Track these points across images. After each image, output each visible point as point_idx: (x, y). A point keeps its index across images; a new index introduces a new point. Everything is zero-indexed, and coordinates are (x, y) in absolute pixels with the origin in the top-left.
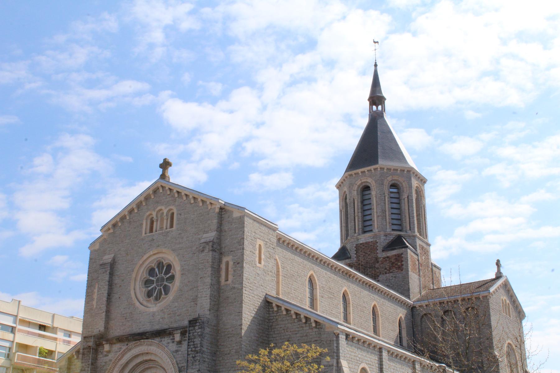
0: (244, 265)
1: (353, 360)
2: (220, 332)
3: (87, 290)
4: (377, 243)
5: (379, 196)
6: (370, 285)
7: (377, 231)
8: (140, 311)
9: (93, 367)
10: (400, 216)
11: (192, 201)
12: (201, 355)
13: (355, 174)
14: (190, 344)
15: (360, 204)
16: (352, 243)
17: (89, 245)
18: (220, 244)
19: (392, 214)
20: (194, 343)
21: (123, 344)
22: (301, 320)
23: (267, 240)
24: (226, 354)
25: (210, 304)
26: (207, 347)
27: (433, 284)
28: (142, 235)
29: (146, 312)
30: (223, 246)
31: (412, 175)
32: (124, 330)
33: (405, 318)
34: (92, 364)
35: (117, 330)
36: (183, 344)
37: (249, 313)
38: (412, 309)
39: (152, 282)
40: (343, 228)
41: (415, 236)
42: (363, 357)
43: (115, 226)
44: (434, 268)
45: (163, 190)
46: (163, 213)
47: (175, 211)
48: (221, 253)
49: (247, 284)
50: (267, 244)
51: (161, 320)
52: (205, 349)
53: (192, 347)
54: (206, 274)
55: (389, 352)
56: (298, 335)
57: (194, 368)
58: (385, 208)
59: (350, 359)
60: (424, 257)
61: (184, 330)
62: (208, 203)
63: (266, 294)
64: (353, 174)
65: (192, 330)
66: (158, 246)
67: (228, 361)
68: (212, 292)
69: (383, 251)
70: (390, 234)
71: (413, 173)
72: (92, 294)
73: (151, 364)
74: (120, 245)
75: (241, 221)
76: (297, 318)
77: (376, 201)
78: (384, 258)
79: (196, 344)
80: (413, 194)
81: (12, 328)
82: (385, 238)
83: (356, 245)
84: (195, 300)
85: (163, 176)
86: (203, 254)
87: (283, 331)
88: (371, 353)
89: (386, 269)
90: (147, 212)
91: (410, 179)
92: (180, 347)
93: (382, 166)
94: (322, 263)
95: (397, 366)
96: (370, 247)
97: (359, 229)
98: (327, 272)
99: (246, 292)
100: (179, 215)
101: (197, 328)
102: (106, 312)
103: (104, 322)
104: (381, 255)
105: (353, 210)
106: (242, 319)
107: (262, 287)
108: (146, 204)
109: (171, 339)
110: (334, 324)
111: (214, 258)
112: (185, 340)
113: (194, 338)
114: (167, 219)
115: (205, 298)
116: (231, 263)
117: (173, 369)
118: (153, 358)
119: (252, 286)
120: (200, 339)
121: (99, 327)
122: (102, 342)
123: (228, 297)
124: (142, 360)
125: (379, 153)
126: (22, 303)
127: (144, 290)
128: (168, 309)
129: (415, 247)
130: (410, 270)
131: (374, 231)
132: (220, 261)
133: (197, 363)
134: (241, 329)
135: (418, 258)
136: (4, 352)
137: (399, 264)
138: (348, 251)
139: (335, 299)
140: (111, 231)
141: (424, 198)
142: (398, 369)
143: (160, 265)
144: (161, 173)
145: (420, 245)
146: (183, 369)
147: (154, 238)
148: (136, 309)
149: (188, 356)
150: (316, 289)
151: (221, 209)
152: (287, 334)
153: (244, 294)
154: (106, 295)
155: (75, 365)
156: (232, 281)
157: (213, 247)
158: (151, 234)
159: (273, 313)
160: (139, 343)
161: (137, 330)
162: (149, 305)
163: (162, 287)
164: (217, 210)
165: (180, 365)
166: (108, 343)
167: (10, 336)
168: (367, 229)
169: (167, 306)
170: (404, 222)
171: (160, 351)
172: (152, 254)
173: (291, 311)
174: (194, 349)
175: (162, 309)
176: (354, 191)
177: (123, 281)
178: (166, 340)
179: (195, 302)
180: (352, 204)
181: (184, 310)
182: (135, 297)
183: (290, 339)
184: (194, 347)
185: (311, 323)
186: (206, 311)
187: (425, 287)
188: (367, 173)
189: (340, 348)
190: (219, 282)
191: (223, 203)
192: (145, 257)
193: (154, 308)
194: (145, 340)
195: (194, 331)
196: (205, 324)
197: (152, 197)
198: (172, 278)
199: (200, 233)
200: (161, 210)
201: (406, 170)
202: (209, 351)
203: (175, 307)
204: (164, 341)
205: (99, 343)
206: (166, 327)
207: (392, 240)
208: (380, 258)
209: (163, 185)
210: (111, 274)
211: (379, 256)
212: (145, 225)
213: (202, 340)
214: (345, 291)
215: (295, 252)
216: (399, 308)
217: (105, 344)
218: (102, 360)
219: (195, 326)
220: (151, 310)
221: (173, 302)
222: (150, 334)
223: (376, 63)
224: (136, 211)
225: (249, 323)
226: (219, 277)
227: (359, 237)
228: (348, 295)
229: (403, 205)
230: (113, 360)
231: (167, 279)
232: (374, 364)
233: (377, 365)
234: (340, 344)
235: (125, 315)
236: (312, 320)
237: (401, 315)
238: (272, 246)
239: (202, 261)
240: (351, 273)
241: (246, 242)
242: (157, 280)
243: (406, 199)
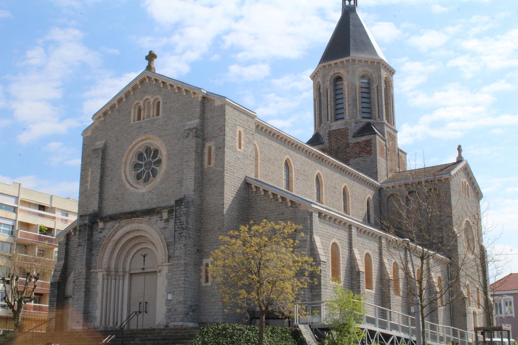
0: (226, 150)
1: (325, 236)
2: (204, 211)
3: (81, 173)
4: (348, 129)
5: (351, 86)
6: (341, 169)
7: (348, 118)
9: (89, 242)
10: (369, 104)
11: (177, 91)
12: (187, 231)
13: (328, 65)
14: (177, 221)
15: (332, 94)
16: (325, 129)
17: (81, 132)
18: (203, 131)
19: (362, 102)
21: (115, 222)
22: (277, 200)
23: (247, 127)
24: (209, 231)
25: (195, 185)
26: (192, 224)
27: (399, 167)
28: (130, 122)
30: (206, 132)
31: (382, 66)
32: (116, 209)
33: (373, 198)
34: (88, 240)
35: (110, 210)
37: (230, 194)
38: (380, 190)
39: (141, 166)
40: (317, 115)
41: (383, 124)
42: (333, 233)
43: (105, 114)
44: (400, 153)
45: (149, 81)
46: (150, 102)
47: (161, 100)
48: (204, 139)
49: (228, 167)
50: (246, 131)
51: (150, 200)
52: (190, 226)
53: (178, 224)
54: (190, 158)
55: (357, 228)
56: (275, 213)
58: (356, 97)
59: (323, 235)
60: (391, 143)
61: (171, 209)
62: (191, 92)
63: (246, 176)
64: (326, 65)
65: (178, 209)
66: (146, 133)
67: (211, 237)
68: (196, 175)
69: (354, 137)
70: (360, 122)
71: (383, 64)
72: (86, 177)
73: (142, 240)
74: (111, 132)
75: (222, 109)
76: (274, 198)
77: (348, 91)
78: (354, 144)
80: (382, 84)
81: (15, 208)
82: (355, 125)
83: (329, 131)
84: (180, 182)
85: (149, 68)
86: (187, 140)
87: (261, 210)
88: (342, 229)
89: (356, 153)
90: (135, 101)
91: (380, 70)
92: (167, 224)
93: (354, 58)
94: (297, 148)
95: (365, 241)
96: (342, 133)
97: (331, 117)
98: (302, 156)
99: (228, 175)
100: (164, 104)
101: (182, 207)
102: (99, 193)
103: (98, 202)
104: (352, 141)
105: (326, 100)
106: (224, 199)
107: (242, 170)
108: (134, 94)
110: (308, 203)
111: (197, 144)
112: (172, 218)
113: (180, 217)
114: (154, 108)
115: (190, 180)
116: (213, 148)
117: (161, 244)
118: (143, 234)
119: (233, 169)
120: (185, 217)
121: (94, 207)
123: (211, 179)
124: (133, 236)
125: (351, 46)
126: (22, 186)
127: (133, 173)
129: (383, 133)
130: (378, 154)
131: (345, 119)
132: (203, 146)
133: (184, 238)
134: (223, 208)
135: (386, 143)
136: (8, 229)
137: (368, 149)
138: (321, 136)
139: (309, 181)
140: (102, 119)
141: (393, 88)
142: (366, 244)
143: (148, 150)
144: (147, 65)
145: (388, 131)
147: (142, 125)
149: (176, 233)
150: (292, 171)
151: (204, 98)
152: (265, 212)
153: (225, 177)
154: (99, 177)
155: (72, 241)
156: (215, 165)
157: (196, 133)
158: (139, 121)
159: (252, 194)
162: (139, 187)
163: (150, 170)
164: (200, 99)
165: (168, 241)
167: (13, 216)
168: (339, 116)
170: (373, 110)
171: (150, 228)
172: (140, 140)
173: (268, 191)
174: (180, 226)
176: (327, 81)
177: (114, 165)
178: (155, 218)
179: (181, 184)
180: (326, 93)
181: (171, 191)
182: (125, 179)
183: (268, 217)
185: (287, 203)
187: (391, 170)
188: (339, 64)
189: (313, 225)
190: (202, 166)
191: (206, 92)
192: (134, 143)
193: (143, 189)
195: (180, 210)
196: (191, 204)
197: (140, 87)
198: (159, 162)
199: (184, 121)
200: (148, 99)
201: (376, 62)
202: (194, 228)
203: (163, 188)
206: (154, 206)
207: (362, 127)
208: (351, 143)
209: (149, 76)
210: (103, 159)
211: (350, 141)
212: (133, 114)
213: (187, 218)
214: (319, 173)
215: (272, 138)
216: (367, 189)
218: (97, 236)
220: (141, 191)
221: (161, 184)
224: (124, 100)
225: (230, 203)
226: (202, 160)
227: (332, 124)
228: (321, 178)
229: (372, 95)
230: (107, 236)
231: (154, 162)
232: (344, 239)
233: (347, 240)
234: (314, 222)
235: (117, 196)
236: (288, 200)
237: (369, 195)
238: (251, 132)
239: (187, 146)
240: (324, 157)
241: (227, 129)
242: (146, 164)
243: (376, 89)
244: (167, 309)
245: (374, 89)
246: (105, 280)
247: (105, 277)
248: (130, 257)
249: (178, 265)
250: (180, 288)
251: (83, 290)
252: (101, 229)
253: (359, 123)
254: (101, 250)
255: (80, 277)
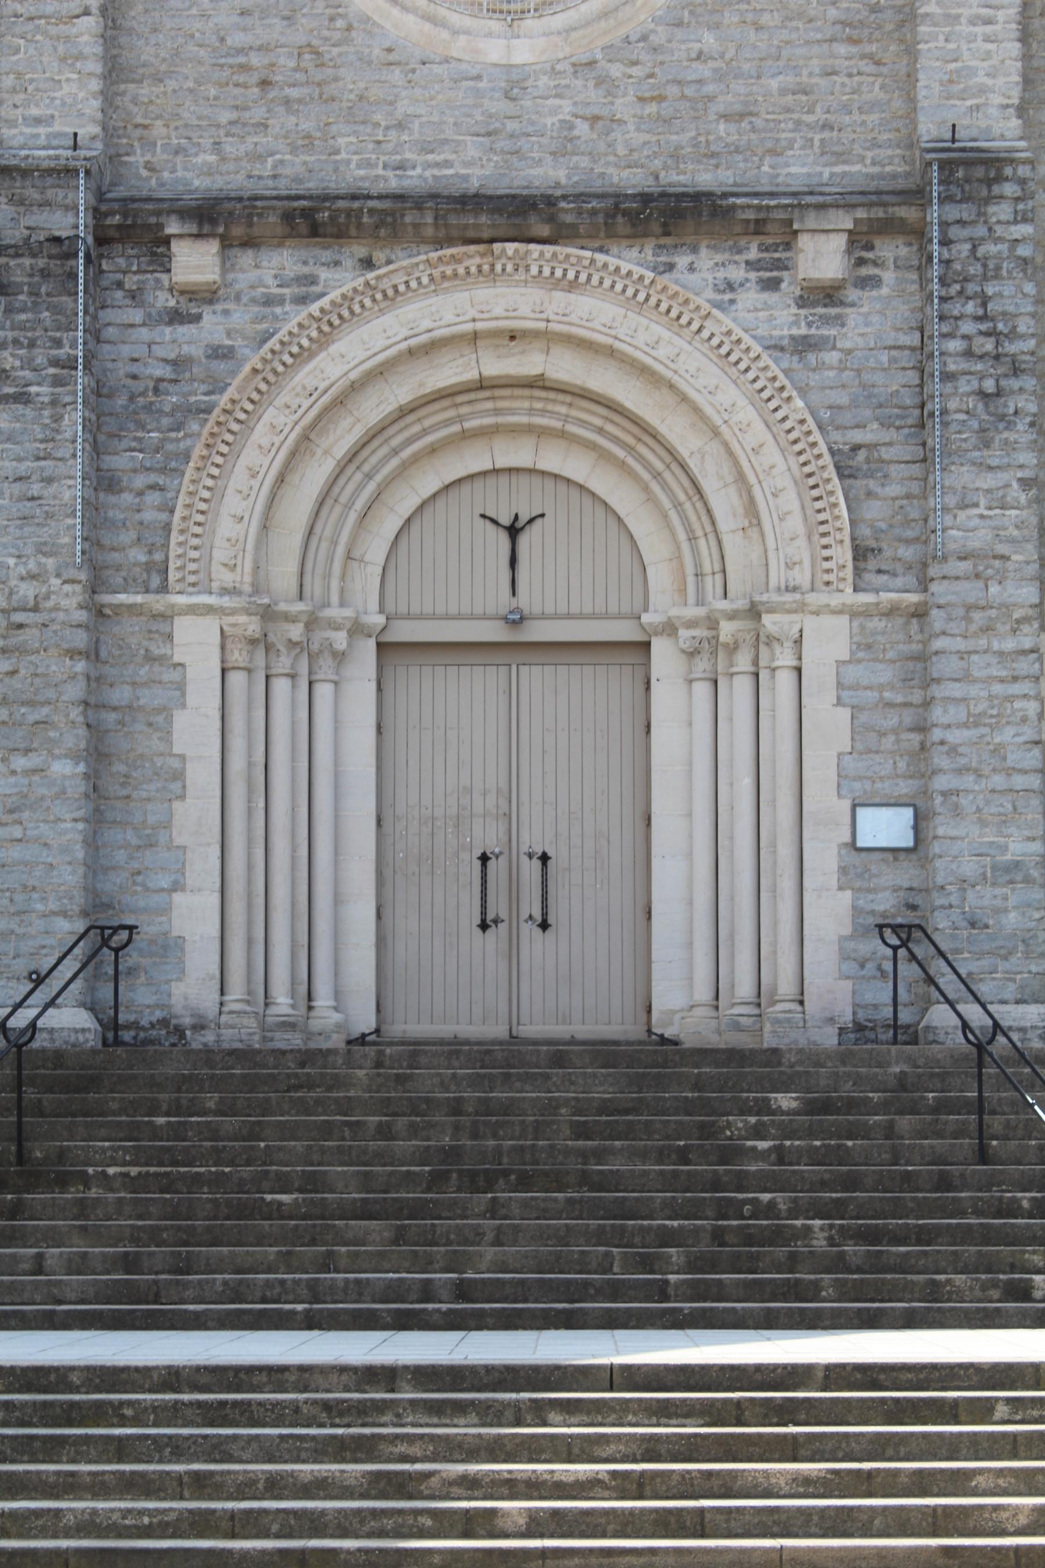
8: (389, 50)
20: (984, 305)
21: (326, 255)
29: (447, 60)
36: (853, 305)
51: (582, 128)
53: (968, 327)
57: (995, 462)
79: (1004, 314)
92: (826, 320)
101: (1002, 211)
109: (747, 263)
113: (985, 278)
115: (980, 30)
122: (153, 220)
128: (635, 63)
146: (868, 461)
148: (349, 28)
160: (477, 260)
161: (380, 171)
166: (212, 235)
169: (627, 40)
175: (584, 58)
181: (774, 84)
184: (987, 334)
186: (993, 111)
194: (532, 246)
195: (981, 231)
204: (691, 268)
205: (119, 227)
217: (180, 236)
219: (988, 200)
221: (679, 24)
222: (594, 212)
235: (255, 60)
244: (857, 911)
246: (236, 679)
247: (238, 656)
248: (390, 524)
249: (977, 616)
250: (1010, 771)
251: (76, 738)
252: (191, 293)
254: (199, 450)
255: (30, 637)
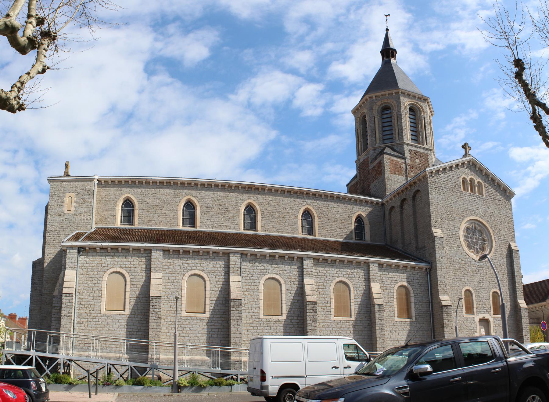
78: (372, 169)
82: (373, 152)
129: (403, 153)
223: (387, 28)
243: (395, 115)
245: (394, 116)
253: (378, 149)
